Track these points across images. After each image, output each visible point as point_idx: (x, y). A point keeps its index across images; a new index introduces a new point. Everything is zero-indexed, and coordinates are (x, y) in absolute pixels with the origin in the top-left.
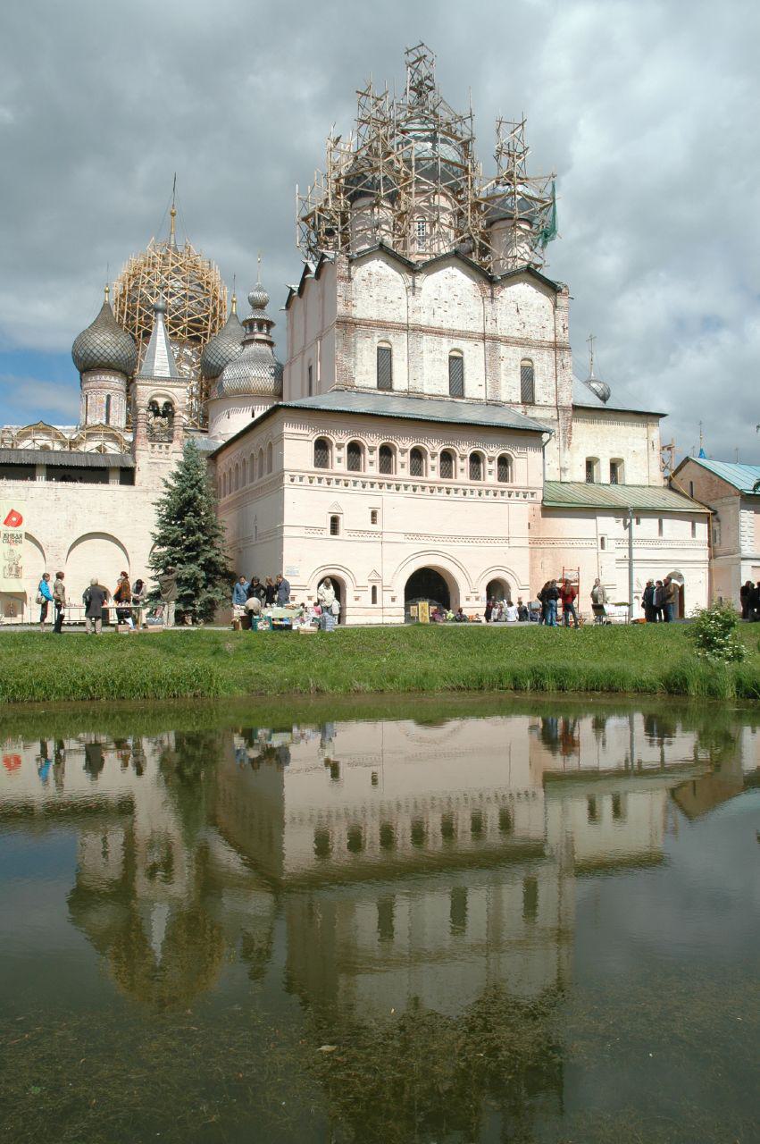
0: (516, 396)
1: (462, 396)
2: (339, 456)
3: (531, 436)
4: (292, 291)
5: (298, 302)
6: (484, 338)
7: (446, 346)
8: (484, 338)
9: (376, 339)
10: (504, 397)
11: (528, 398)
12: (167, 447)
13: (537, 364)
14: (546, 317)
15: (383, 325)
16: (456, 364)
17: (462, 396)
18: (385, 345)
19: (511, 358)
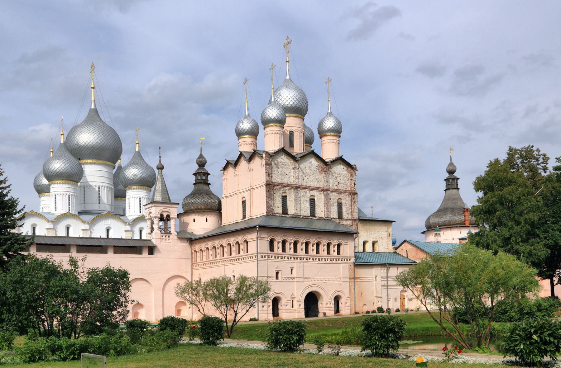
0: (336, 216)
1: (315, 216)
2: (277, 246)
3: (350, 235)
4: (228, 164)
5: (231, 169)
6: (323, 190)
8: (323, 190)
9: (281, 192)
10: (332, 216)
11: (340, 217)
13: (343, 201)
15: (284, 185)
16: (312, 201)
17: (315, 216)
18: (284, 194)
19: (334, 197)
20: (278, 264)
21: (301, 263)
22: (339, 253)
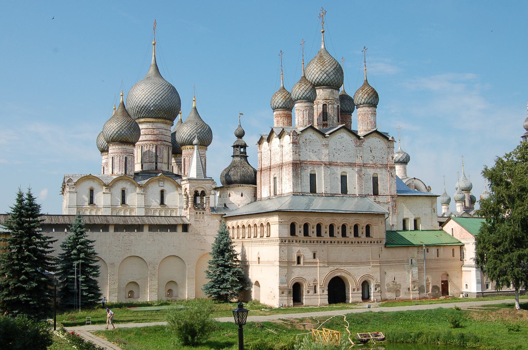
2: (299, 230)
4: (262, 139)
7: (339, 171)
9: (309, 170)
12: (203, 213)
14: (384, 153)
15: (312, 163)
16: (344, 178)
18: (313, 173)
20: (299, 248)
21: (325, 247)
22: (368, 235)
